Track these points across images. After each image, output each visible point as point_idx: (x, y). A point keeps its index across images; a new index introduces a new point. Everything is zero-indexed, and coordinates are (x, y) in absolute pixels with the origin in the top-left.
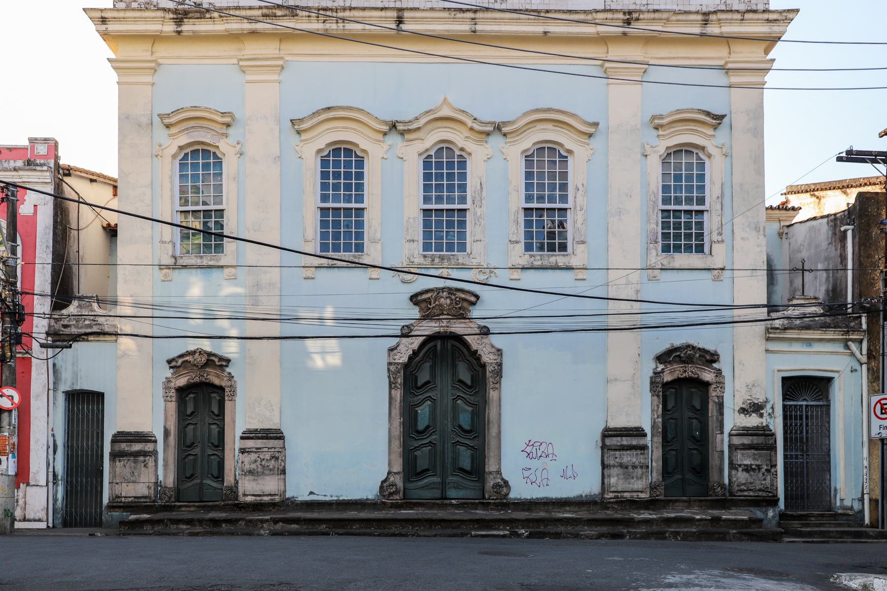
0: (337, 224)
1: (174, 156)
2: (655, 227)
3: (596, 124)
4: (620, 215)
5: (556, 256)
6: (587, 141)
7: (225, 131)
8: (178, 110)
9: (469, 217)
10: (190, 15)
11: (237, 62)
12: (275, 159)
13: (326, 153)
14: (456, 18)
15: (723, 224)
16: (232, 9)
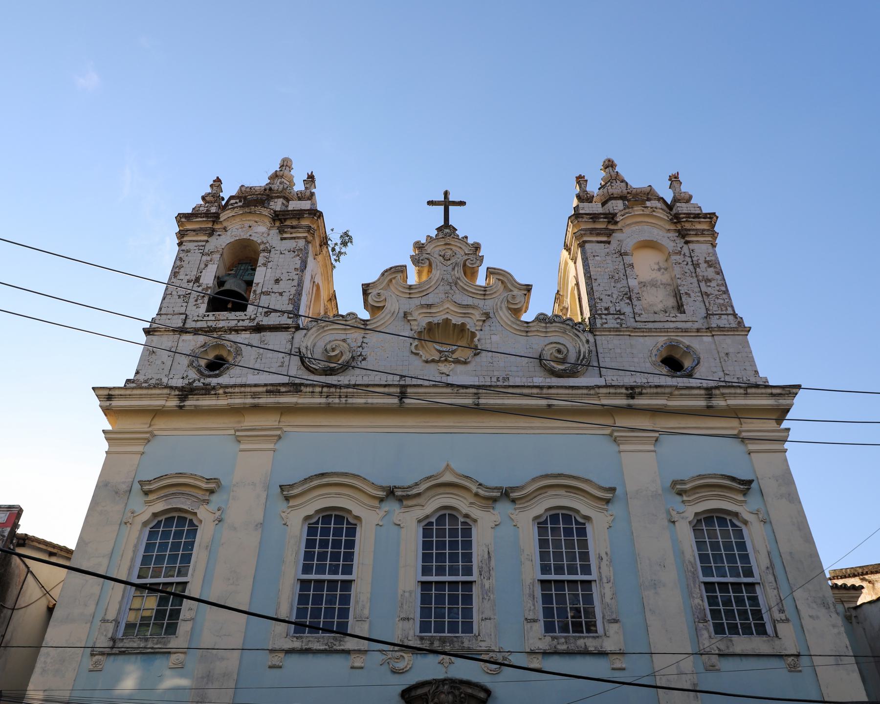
0: (318, 599)
1: (145, 524)
2: (701, 602)
3: (612, 490)
4: (655, 588)
5: (584, 638)
6: (605, 507)
7: (207, 498)
8: (162, 476)
9: (476, 591)
10: (196, 392)
11: (234, 433)
12: (257, 526)
13: (314, 520)
14: (459, 393)
15: (782, 599)
16: (238, 386)
